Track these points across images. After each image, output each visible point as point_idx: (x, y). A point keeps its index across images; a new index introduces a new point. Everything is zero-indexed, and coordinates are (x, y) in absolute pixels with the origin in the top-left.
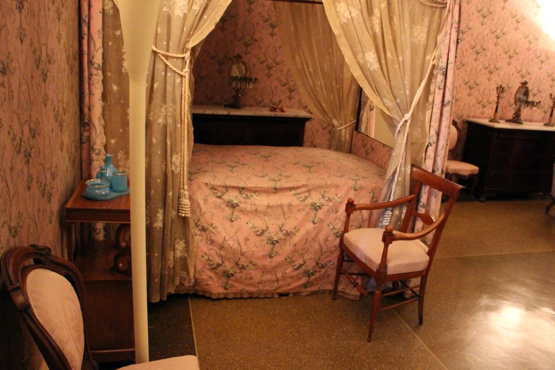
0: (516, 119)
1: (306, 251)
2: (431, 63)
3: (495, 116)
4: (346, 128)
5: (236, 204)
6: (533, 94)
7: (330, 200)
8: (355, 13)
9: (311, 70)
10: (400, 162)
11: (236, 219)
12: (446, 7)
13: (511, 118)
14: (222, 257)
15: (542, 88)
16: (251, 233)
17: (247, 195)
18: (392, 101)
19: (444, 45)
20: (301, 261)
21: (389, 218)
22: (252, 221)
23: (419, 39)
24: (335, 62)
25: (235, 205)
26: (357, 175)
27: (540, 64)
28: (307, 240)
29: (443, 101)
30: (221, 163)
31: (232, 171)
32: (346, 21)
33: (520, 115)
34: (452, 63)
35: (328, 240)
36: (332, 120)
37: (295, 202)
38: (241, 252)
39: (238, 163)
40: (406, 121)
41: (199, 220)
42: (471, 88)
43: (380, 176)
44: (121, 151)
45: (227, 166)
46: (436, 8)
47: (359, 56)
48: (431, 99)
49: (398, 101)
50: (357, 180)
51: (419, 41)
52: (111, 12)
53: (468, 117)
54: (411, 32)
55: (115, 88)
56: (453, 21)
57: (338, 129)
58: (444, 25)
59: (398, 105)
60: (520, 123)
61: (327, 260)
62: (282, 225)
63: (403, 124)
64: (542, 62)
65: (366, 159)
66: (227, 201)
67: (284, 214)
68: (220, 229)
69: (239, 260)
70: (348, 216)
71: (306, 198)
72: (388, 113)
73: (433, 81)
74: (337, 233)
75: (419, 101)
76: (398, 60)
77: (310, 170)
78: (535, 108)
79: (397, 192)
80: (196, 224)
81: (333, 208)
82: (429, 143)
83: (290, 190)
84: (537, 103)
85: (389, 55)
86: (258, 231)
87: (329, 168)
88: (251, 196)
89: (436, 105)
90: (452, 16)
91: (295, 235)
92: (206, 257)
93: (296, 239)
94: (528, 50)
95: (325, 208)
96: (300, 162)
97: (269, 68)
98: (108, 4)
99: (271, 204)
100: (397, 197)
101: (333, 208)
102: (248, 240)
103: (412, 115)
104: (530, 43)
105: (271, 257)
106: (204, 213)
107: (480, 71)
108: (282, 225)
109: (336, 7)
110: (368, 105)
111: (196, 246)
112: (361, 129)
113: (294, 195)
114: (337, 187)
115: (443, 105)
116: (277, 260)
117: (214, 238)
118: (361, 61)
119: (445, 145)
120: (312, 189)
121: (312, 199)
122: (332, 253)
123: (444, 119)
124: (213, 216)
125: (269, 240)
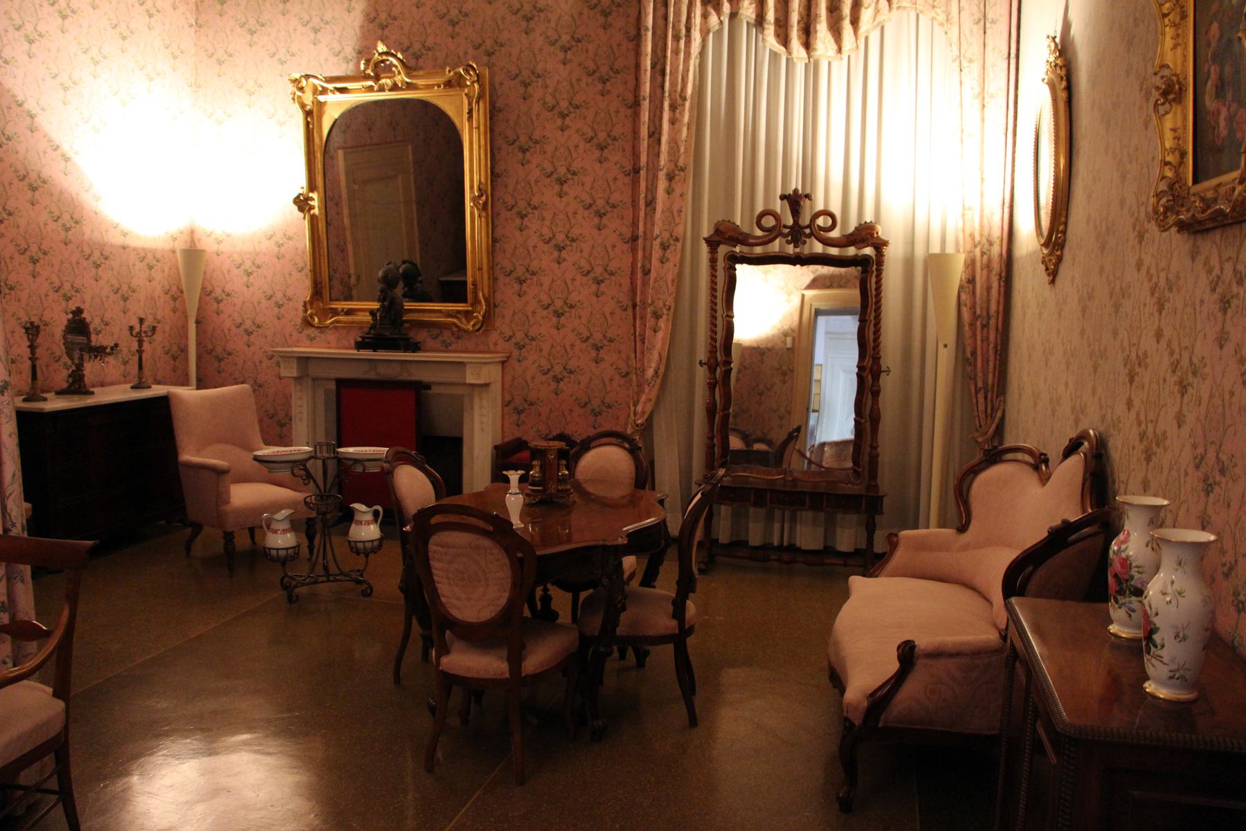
0: (77, 385)
3: (33, 388)
6: (95, 329)
13: (65, 385)
15: (108, 316)
27: (94, 270)
33: (84, 375)
60: (85, 392)
64: (98, 266)
78: (110, 359)
84: (112, 349)
94: (66, 244)
104: (67, 230)
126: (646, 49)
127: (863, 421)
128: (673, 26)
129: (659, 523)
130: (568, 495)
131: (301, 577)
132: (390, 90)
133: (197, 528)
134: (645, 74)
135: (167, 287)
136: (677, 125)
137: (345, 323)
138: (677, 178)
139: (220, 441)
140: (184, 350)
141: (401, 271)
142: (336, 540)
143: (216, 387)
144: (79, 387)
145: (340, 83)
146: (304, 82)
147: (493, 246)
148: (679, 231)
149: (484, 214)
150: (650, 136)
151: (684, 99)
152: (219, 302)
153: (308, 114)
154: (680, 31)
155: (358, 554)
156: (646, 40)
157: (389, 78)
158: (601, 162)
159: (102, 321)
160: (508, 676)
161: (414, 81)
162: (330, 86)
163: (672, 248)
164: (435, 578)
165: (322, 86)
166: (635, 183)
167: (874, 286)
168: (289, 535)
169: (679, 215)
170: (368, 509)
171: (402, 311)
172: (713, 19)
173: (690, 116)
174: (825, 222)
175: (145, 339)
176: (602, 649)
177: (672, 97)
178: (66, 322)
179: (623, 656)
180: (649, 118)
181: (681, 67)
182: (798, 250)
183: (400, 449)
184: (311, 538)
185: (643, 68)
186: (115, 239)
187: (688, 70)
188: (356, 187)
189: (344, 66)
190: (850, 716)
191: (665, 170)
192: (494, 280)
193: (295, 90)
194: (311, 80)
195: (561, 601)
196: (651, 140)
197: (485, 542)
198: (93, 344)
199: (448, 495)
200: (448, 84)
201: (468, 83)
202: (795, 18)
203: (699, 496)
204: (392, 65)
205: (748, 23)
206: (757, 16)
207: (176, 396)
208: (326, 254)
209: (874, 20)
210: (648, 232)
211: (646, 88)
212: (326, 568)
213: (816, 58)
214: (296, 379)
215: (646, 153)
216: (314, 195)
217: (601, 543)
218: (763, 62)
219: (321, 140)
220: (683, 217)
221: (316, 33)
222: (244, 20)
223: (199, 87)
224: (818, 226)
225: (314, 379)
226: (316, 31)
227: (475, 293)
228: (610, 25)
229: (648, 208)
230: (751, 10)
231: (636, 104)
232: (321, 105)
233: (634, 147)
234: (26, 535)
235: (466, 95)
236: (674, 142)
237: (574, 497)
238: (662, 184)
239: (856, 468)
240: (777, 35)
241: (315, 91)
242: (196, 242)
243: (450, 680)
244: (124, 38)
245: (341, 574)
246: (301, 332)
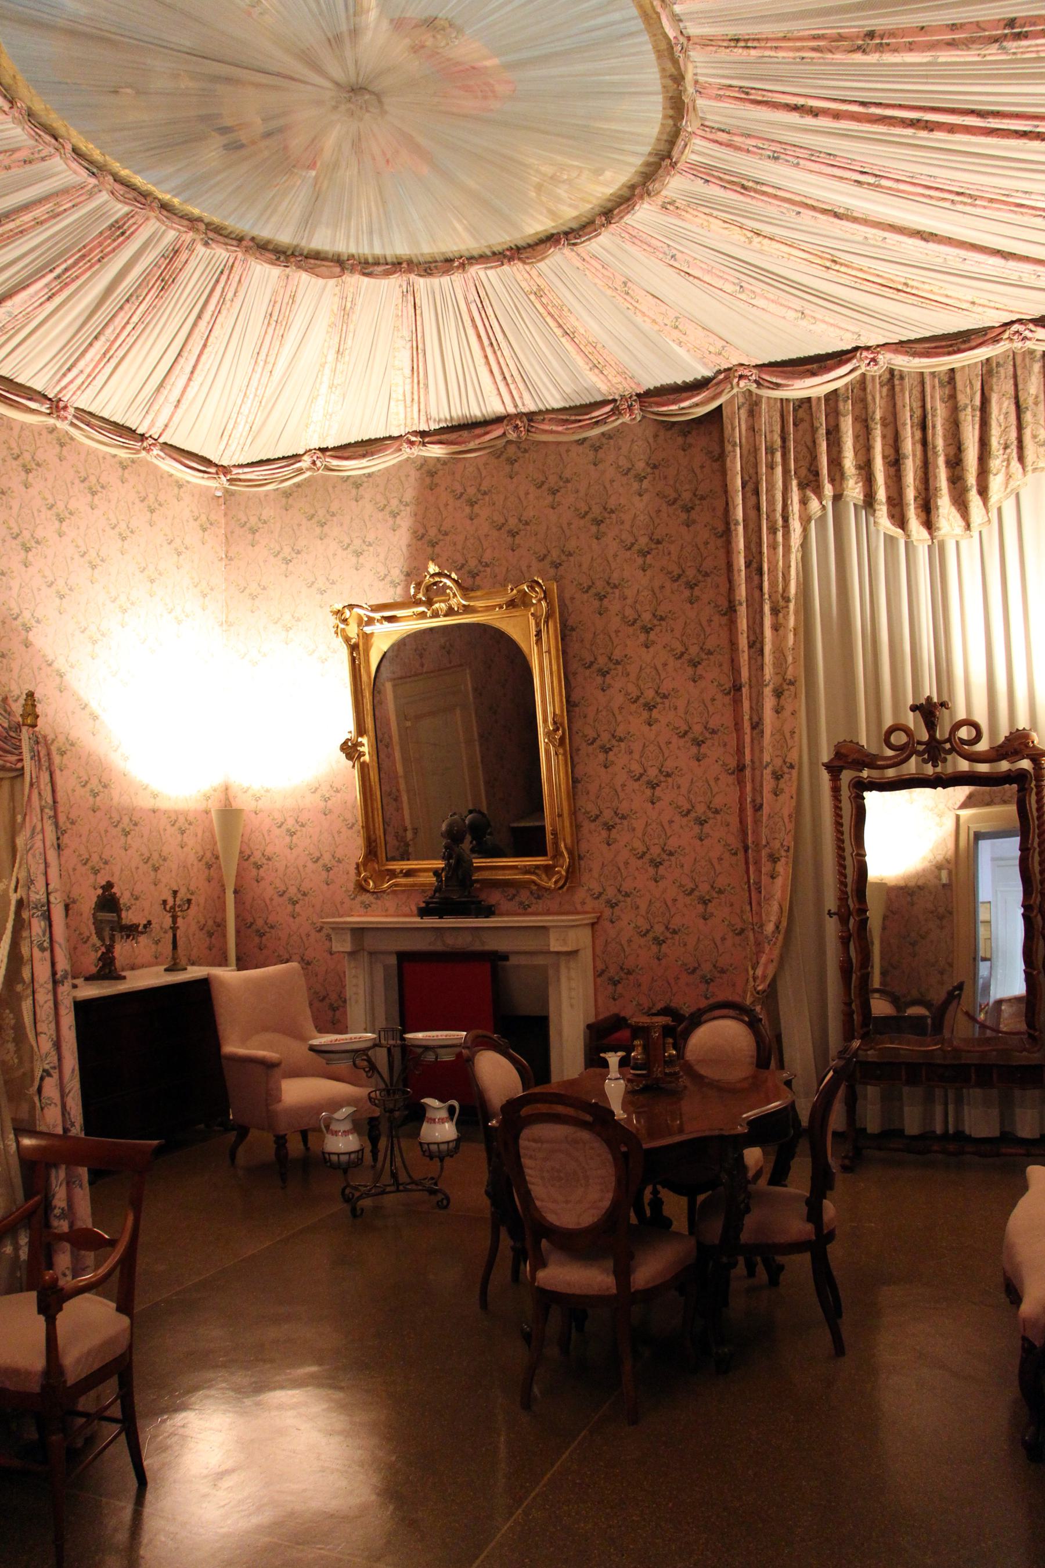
0: (107, 970)
2: (14, 898)
12: (23, 774)
13: (94, 970)
15: (138, 888)
19: (34, 856)
29: (54, 973)
34: (56, 891)
48: (26, 974)
64: (127, 834)
73: (25, 934)
78: (143, 939)
82: (44, 1071)
84: (145, 926)
89: (41, 986)
90: (40, 794)
104: (95, 795)
115: (55, 983)
126: (737, 546)
127: (1035, 973)
128: (768, 516)
129: (785, 1108)
130: (677, 1079)
131: (366, 1186)
132: (445, 615)
133: (243, 1131)
134: (739, 576)
135: (201, 853)
136: (781, 632)
137: (405, 885)
138: (786, 693)
139: (265, 1029)
140: (221, 925)
141: (467, 822)
142: (404, 1143)
143: (257, 967)
144: (110, 972)
145: (387, 611)
146: (347, 612)
147: (573, 788)
148: (793, 757)
149: (561, 751)
150: (750, 647)
151: (787, 600)
152: (258, 867)
153: (353, 648)
154: (776, 522)
155: (431, 1157)
156: (737, 535)
157: (443, 601)
158: (695, 681)
159: (132, 895)
160: (615, 1291)
161: (472, 604)
162: (377, 616)
163: (786, 776)
164: (527, 1178)
165: (368, 616)
166: (737, 702)
167: (1034, 806)
168: (351, 1137)
169: (792, 737)
170: (442, 1105)
171: (471, 869)
172: (814, 505)
173: (796, 620)
174: (969, 732)
175: (179, 914)
176: (725, 1260)
177: (773, 598)
178: (95, 899)
179: (751, 1272)
180: (748, 626)
181: (781, 563)
182: (939, 769)
183: (480, 1032)
184: (374, 1141)
185: (735, 568)
186: (145, 802)
187: (789, 567)
188: (408, 724)
189: (392, 591)
190: (1029, 1334)
191: (771, 686)
192: (577, 827)
193: (338, 622)
194: (356, 610)
195: (675, 1206)
196: (753, 650)
197: (585, 1135)
198: (124, 922)
199: (536, 1085)
200: (511, 604)
201: (534, 601)
202: (910, 494)
203: (831, 1073)
204: (446, 587)
205: (855, 505)
206: (865, 496)
207: (216, 977)
208: (380, 806)
209: (1006, 487)
210: (756, 760)
211: (742, 592)
212: (394, 1175)
213: (940, 538)
214: (352, 954)
215: (747, 666)
216: (364, 740)
217: (717, 1133)
218: (877, 547)
219: (370, 677)
220: (796, 738)
221: (358, 556)
222: (278, 548)
223: (231, 625)
224: (960, 739)
225: (371, 954)
226: (358, 554)
227: (556, 844)
228: (694, 522)
229: (755, 732)
230: (857, 490)
231: (731, 609)
232: (367, 637)
233: (732, 661)
234: (83, 1135)
235: (532, 614)
236: (780, 653)
237: (684, 1081)
238: (769, 702)
239: (1032, 1032)
240: (891, 516)
241: (360, 622)
242: (232, 800)
243: (548, 1298)
244: (152, 581)
245: (413, 1182)
246: (354, 899)
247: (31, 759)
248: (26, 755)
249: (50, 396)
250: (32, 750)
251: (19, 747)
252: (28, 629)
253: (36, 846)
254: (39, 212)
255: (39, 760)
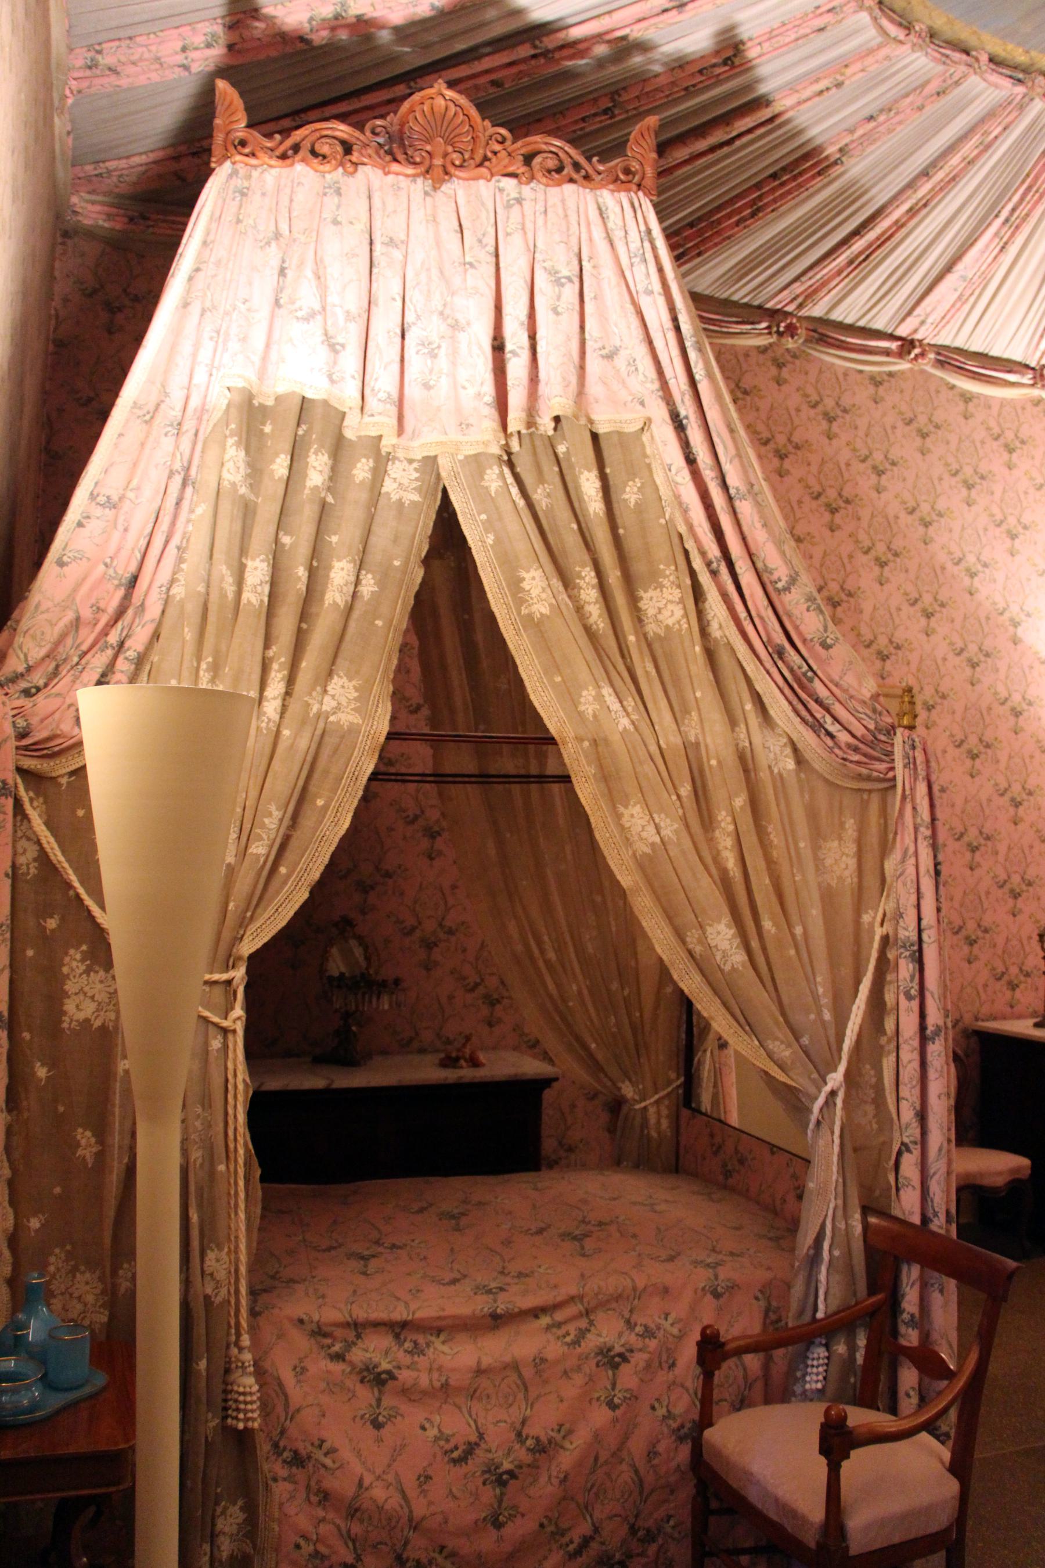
1: (597, 1495)
2: (879, 932)
4: (657, 1102)
5: (389, 1372)
7: (648, 1333)
8: (670, 828)
9: (552, 955)
10: (832, 1206)
11: (390, 1418)
12: (894, 786)
14: (354, 1541)
16: (435, 1456)
17: (416, 1343)
18: (789, 1046)
19: (904, 884)
20: (584, 1528)
21: (821, 1369)
22: (437, 1419)
23: (838, 873)
24: (614, 929)
25: (384, 1376)
26: (714, 1250)
28: (596, 1459)
29: (923, 1027)
30: (330, 1249)
31: (365, 1274)
32: (648, 850)
34: (930, 927)
35: (656, 1454)
36: (620, 1085)
37: (554, 1349)
38: (410, 1520)
39: (377, 1243)
40: (833, 1093)
41: (283, 1432)
42: (971, 942)
43: (777, 1239)
44: (57, 1251)
45: (350, 1256)
46: (870, 791)
47: (692, 937)
48: (889, 1025)
49: (805, 1040)
50: (718, 1264)
51: (841, 879)
52: (33, 871)
53: (977, 1019)
54: (816, 858)
55: (42, 1072)
56: (919, 820)
57: (637, 1107)
58: (896, 833)
59: (806, 1053)
61: (661, 1513)
62: (523, 1423)
63: (826, 1103)
65: (725, 1187)
66: (360, 1365)
67: (526, 1389)
68: (346, 1454)
69: (406, 1544)
70: (708, 1376)
71: (582, 1333)
72: (781, 1077)
73: (889, 977)
74: (679, 1429)
75: (859, 1035)
76: (793, 936)
77: (583, 1248)
79: (832, 1291)
80: (276, 1445)
81: (660, 1356)
82: (903, 1144)
83: (536, 1317)
85: (767, 924)
86: (456, 1448)
87: (634, 1236)
88: (428, 1345)
89: (906, 1042)
90: (914, 808)
91: (562, 1447)
92: (308, 1549)
93: (566, 1460)
95: (639, 1359)
96: (549, 1226)
97: (429, 945)
98: (25, 851)
99: (486, 1361)
100: (835, 1304)
101: (660, 1356)
102: (428, 1478)
103: (847, 1075)
105: (498, 1525)
106: (298, 1410)
107: (988, 893)
108: (523, 1423)
109: (618, 816)
110: (711, 1036)
111: (277, 1515)
112: (699, 1103)
113: (548, 1328)
114: (666, 1291)
115: (924, 1038)
116: (517, 1530)
117: (331, 1483)
118: (698, 949)
119: (945, 1144)
120: (596, 1308)
121: (599, 1335)
122: (672, 1492)
123: (932, 1074)
124: (324, 1416)
125: (489, 1471)
247: (905, 767)
248: (899, 764)
249: (1033, 365)
250: (906, 756)
251: (892, 753)
252: (1016, 624)
253: (908, 871)
254: (968, 149)
255: (915, 768)
